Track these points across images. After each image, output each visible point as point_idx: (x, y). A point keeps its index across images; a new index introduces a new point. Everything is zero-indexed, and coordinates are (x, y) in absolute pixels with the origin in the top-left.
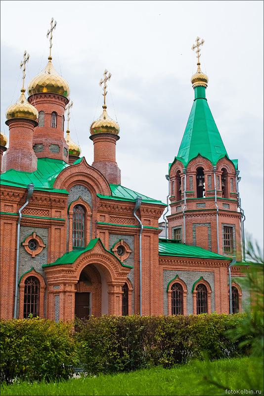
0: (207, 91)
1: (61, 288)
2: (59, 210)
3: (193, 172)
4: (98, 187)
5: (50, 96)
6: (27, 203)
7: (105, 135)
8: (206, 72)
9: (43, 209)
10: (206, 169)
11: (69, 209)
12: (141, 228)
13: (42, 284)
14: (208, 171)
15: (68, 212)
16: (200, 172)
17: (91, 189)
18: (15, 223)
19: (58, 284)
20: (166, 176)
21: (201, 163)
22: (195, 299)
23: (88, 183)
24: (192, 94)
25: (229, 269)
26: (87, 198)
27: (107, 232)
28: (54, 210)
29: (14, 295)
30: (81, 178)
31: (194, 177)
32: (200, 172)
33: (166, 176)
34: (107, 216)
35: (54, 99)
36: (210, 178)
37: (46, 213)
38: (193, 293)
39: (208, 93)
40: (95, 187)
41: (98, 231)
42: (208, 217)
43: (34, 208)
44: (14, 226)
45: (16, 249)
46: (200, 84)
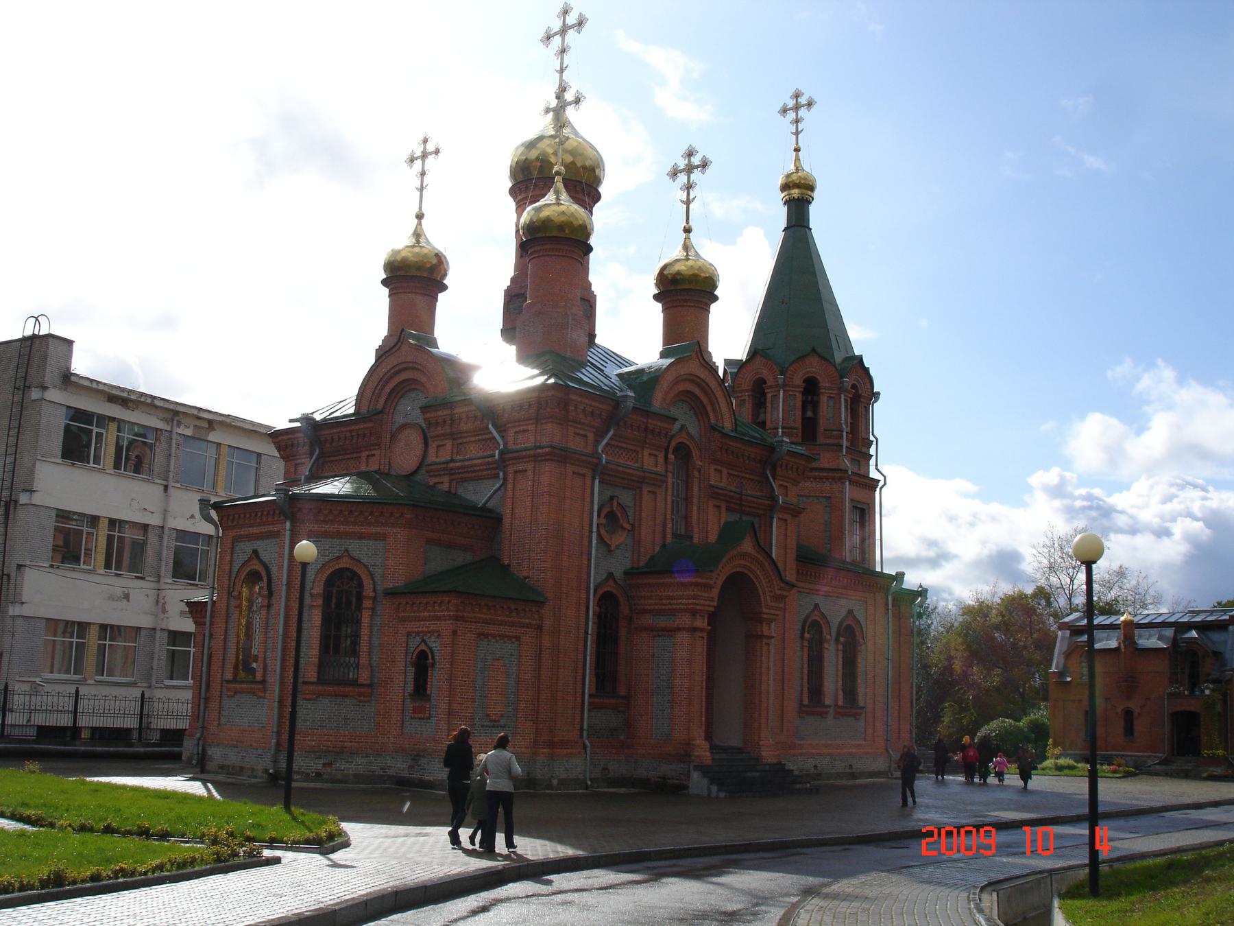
0: (814, 210)
1: (685, 620)
3: (798, 386)
4: (714, 409)
6: (611, 433)
8: (812, 167)
10: (824, 383)
12: (777, 501)
13: (625, 609)
14: (829, 388)
16: (811, 387)
18: (589, 474)
19: (673, 613)
21: (813, 367)
22: (840, 654)
23: (698, 398)
24: (779, 216)
25: (890, 598)
27: (723, 505)
29: (586, 633)
31: (799, 397)
32: (811, 387)
34: (725, 472)
36: (831, 402)
38: (837, 640)
40: (709, 408)
42: (827, 485)
44: (589, 482)
45: (591, 532)
46: (798, 197)
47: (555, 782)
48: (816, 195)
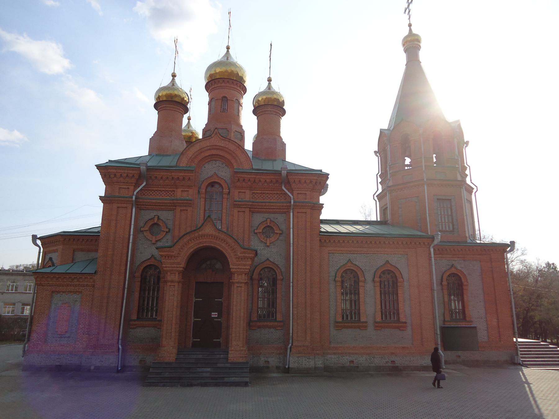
2: (186, 189)
5: (219, 81)
6: (143, 185)
7: (270, 108)
9: (167, 189)
11: (200, 188)
15: (199, 192)
17: (229, 164)
20: (375, 152)
25: (432, 250)
26: (225, 173)
27: (247, 210)
28: (179, 190)
30: (214, 152)
33: (375, 152)
34: (248, 192)
35: (223, 84)
37: (172, 194)
39: (423, 55)
40: (233, 161)
41: (236, 210)
43: (157, 189)
47: (92, 368)
48: (422, 45)
